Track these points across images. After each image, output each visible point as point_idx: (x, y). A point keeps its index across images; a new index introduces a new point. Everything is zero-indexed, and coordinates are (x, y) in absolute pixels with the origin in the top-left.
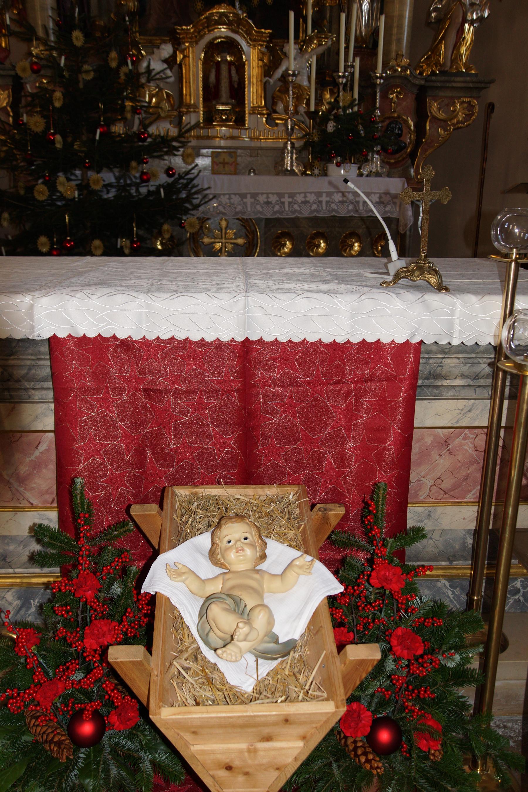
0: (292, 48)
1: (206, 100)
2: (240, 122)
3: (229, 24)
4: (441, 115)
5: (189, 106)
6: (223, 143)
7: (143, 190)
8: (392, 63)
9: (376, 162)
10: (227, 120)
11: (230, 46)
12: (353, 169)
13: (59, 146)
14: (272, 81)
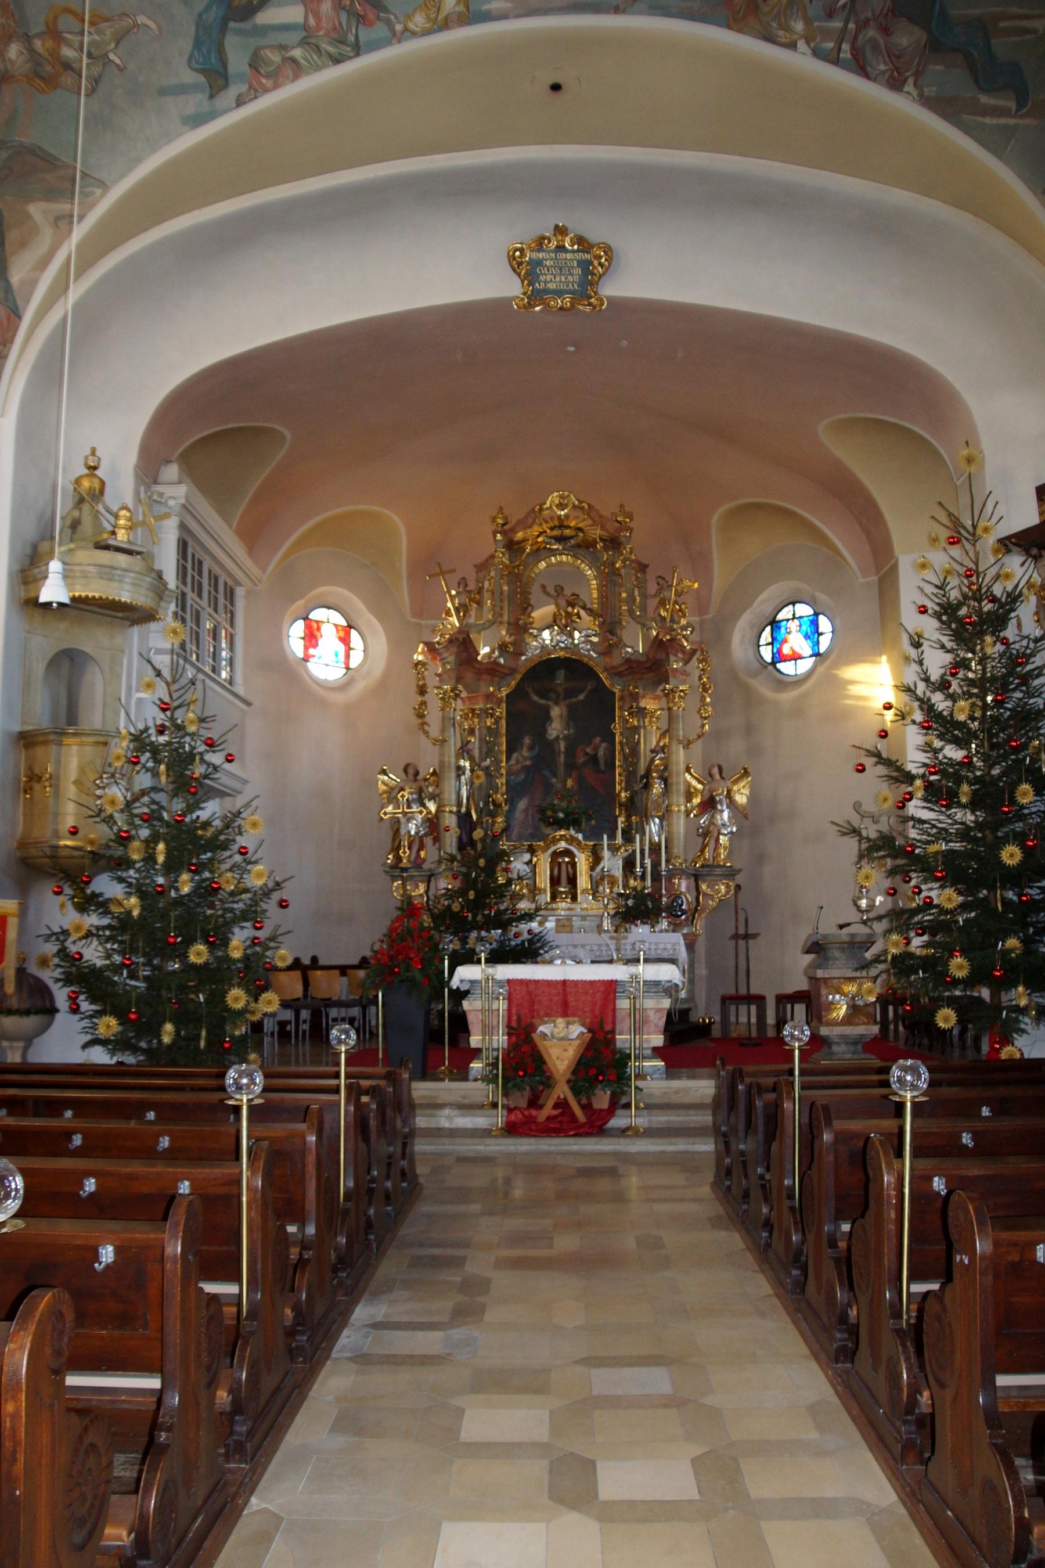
0: (606, 853)
1: (551, 886)
2: (574, 898)
3: (567, 840)
4: (709, 891)
5: (540, 890)
6: (563, 913)
7: (513, 943)
8: (673, 861)
9: (664, 924)
10: (566, 897)
11: (567, 852)
12: (647, 927)
13: (470, 918)
14: (594, 874)
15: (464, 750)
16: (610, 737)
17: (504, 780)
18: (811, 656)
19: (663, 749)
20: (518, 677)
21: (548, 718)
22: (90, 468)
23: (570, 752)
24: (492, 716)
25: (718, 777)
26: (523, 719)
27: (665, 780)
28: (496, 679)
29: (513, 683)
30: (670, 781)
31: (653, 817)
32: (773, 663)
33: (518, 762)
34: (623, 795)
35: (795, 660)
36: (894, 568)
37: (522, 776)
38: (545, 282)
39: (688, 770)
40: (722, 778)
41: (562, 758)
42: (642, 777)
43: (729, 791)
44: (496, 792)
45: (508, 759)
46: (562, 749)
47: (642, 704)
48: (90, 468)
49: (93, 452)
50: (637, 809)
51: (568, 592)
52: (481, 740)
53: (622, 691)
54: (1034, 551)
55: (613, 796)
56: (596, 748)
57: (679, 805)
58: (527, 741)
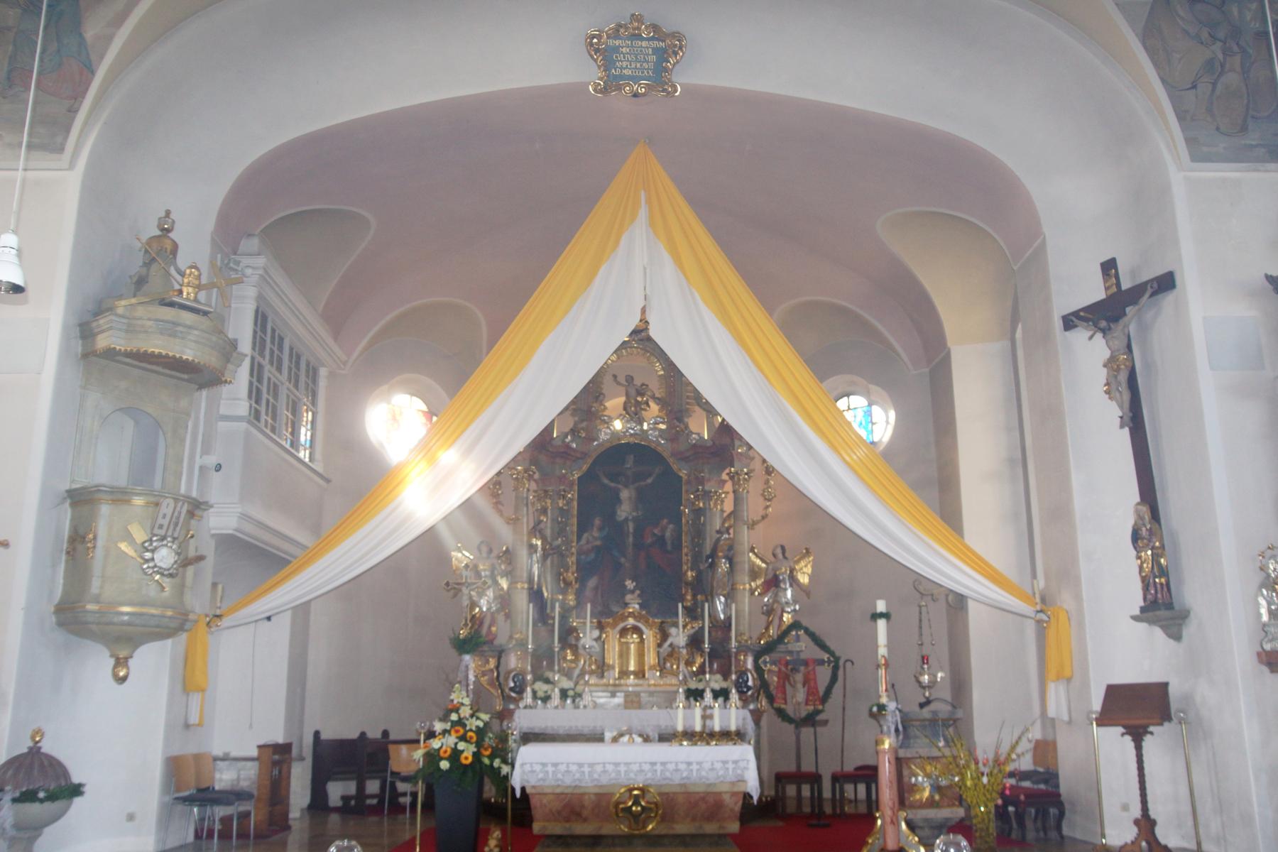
3: (635, 618)
15: (536, 530)
16: (677, 518)
17: (574, 559)
19: (728, 529)
20: (590, 461)
21: (618, 501)
22: (163, 230)
23: (639, 533)
24: (564, 497)
25: (780, 556)
26: (594, 501)
27: (730, 560)
28: (568, 463)
29: (585, 468)
30: (735, 560)
31: (718, 595)
33: (588, 542)
34: (689, 573)
36: (947, 358)
37: (592, 556)
38: (622, 68)
39: (752, 550)
40: (785, 557)
41: (631, 539)
42: (708, 557)
43: (792, 571)
44: (567, 571)
45: (579, 538)
46: (631, 530)
47: (707, 488)
48: (163, 230)
49: (168, 213)
50: (704, 589)
51: (638, 382)
52: (553, 520)
53: (689, 475)
54: (1103, 324)
55: (680, 576)
56: (664, 529)
57: (745, 584)
58: (597, 522)
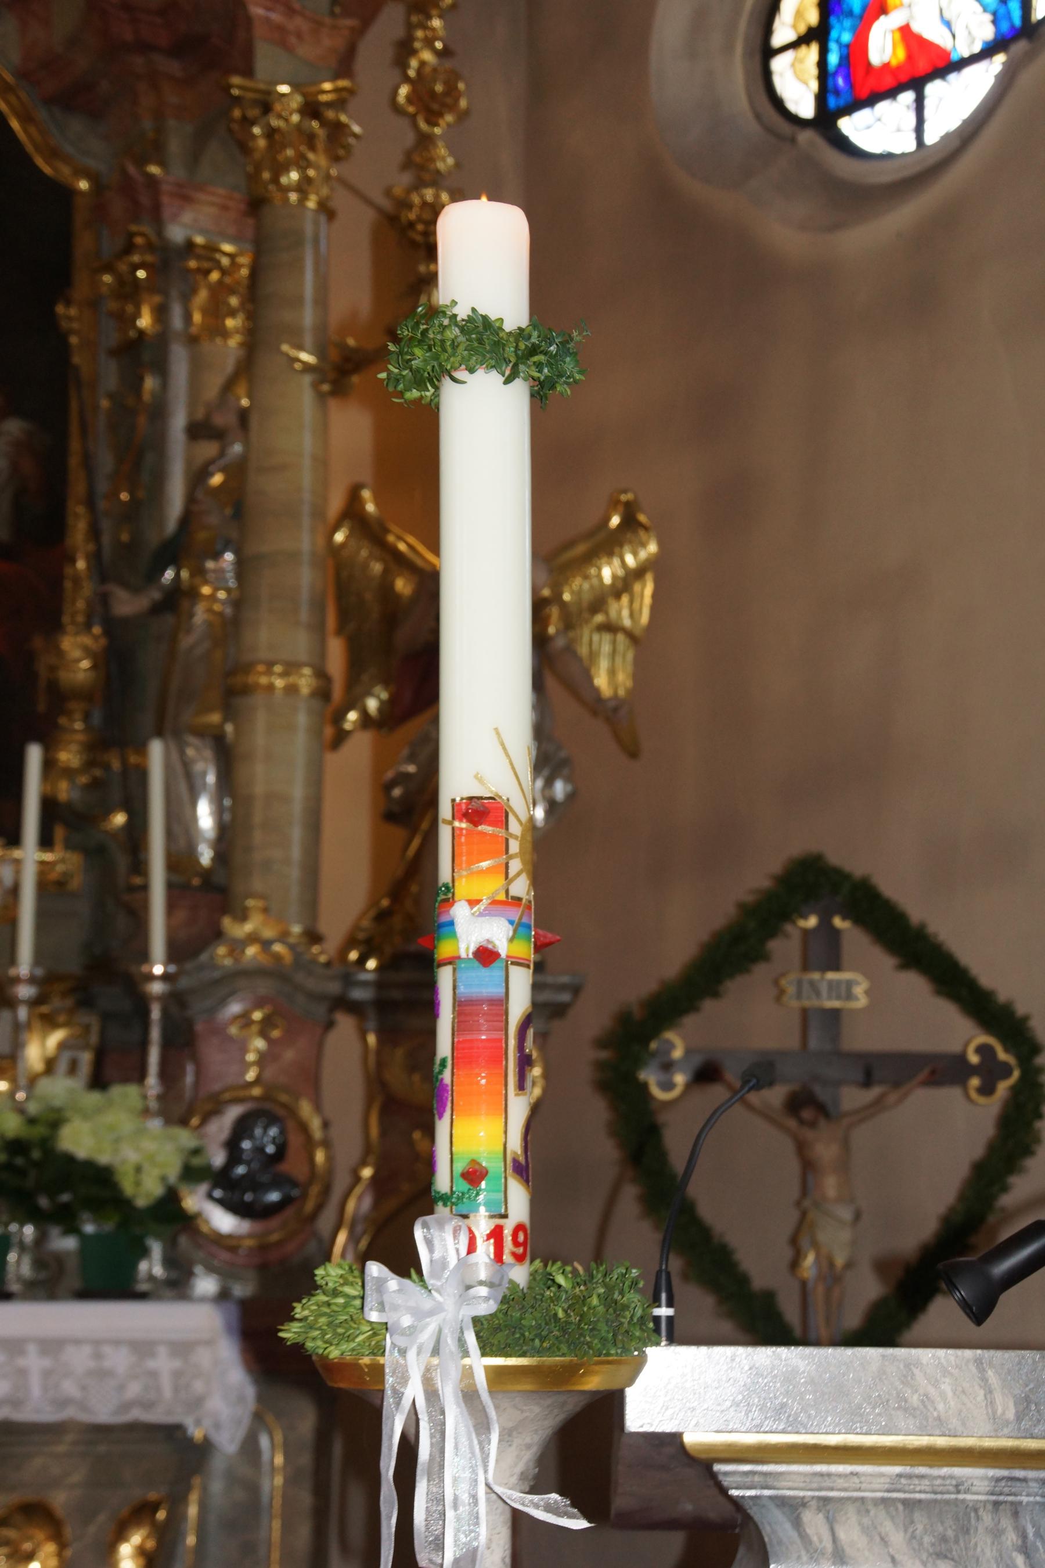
18: (988, 52)
32: (826, 119)
35: (917, 84)
47: (176, 234)
